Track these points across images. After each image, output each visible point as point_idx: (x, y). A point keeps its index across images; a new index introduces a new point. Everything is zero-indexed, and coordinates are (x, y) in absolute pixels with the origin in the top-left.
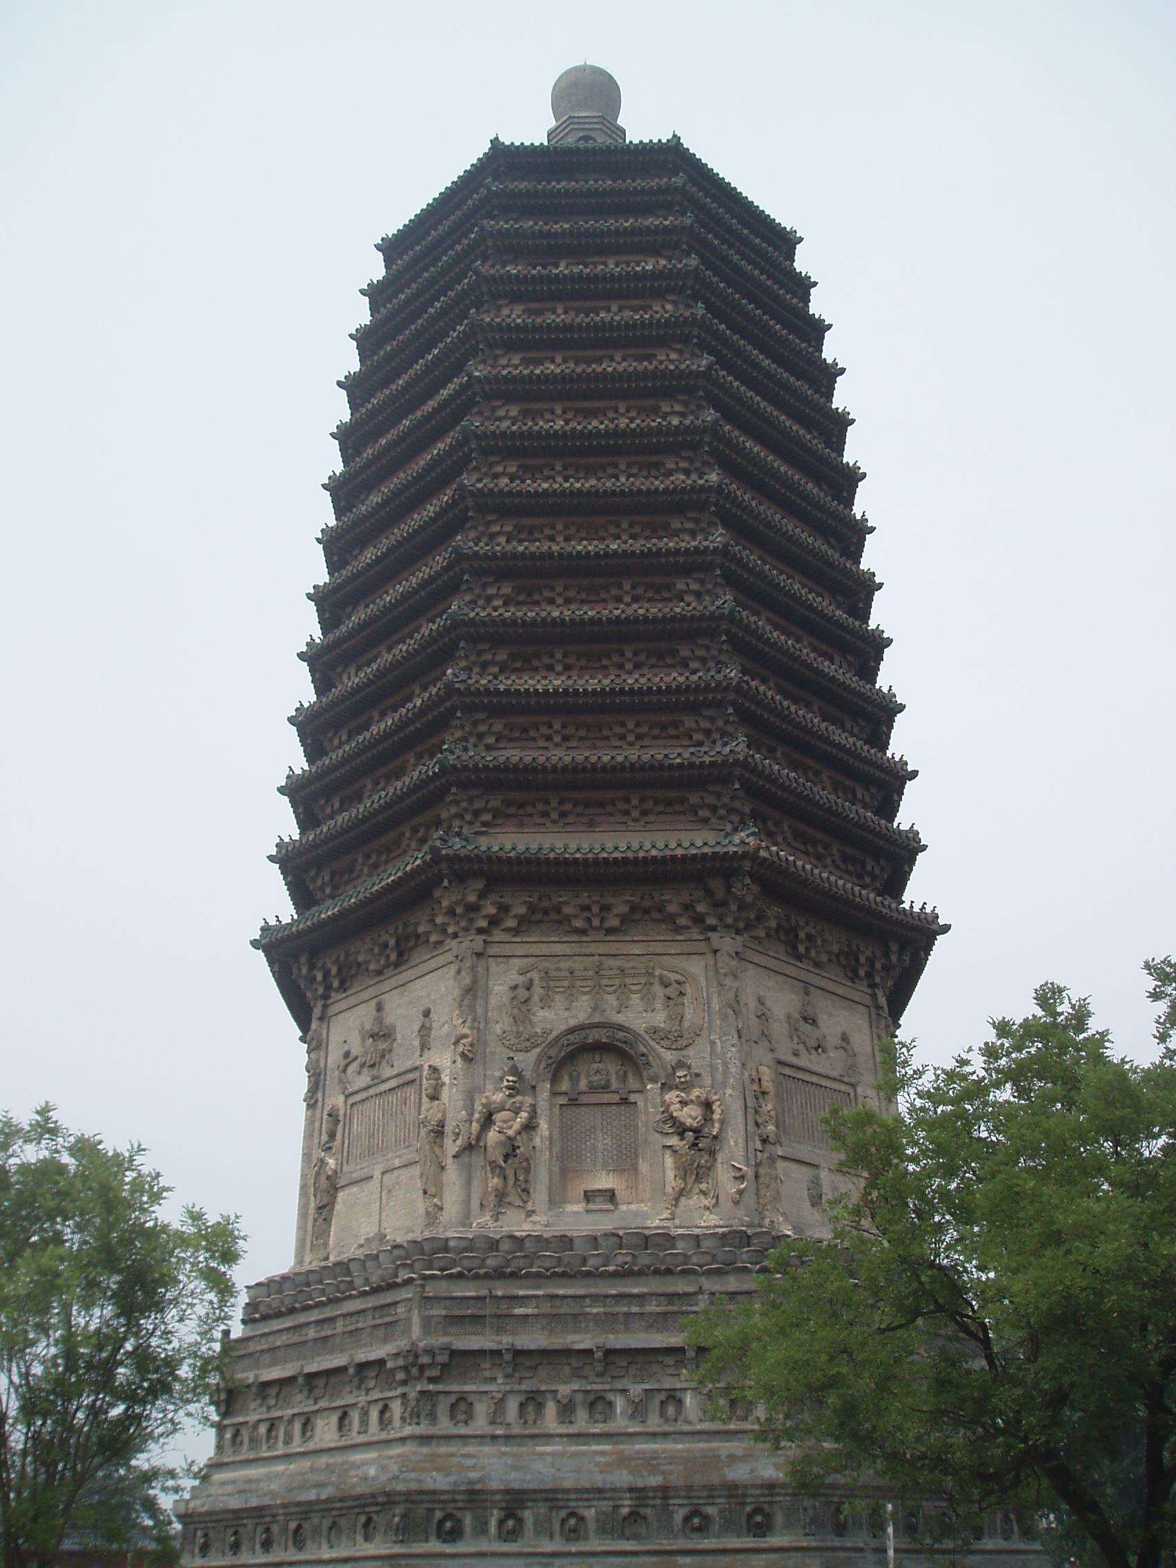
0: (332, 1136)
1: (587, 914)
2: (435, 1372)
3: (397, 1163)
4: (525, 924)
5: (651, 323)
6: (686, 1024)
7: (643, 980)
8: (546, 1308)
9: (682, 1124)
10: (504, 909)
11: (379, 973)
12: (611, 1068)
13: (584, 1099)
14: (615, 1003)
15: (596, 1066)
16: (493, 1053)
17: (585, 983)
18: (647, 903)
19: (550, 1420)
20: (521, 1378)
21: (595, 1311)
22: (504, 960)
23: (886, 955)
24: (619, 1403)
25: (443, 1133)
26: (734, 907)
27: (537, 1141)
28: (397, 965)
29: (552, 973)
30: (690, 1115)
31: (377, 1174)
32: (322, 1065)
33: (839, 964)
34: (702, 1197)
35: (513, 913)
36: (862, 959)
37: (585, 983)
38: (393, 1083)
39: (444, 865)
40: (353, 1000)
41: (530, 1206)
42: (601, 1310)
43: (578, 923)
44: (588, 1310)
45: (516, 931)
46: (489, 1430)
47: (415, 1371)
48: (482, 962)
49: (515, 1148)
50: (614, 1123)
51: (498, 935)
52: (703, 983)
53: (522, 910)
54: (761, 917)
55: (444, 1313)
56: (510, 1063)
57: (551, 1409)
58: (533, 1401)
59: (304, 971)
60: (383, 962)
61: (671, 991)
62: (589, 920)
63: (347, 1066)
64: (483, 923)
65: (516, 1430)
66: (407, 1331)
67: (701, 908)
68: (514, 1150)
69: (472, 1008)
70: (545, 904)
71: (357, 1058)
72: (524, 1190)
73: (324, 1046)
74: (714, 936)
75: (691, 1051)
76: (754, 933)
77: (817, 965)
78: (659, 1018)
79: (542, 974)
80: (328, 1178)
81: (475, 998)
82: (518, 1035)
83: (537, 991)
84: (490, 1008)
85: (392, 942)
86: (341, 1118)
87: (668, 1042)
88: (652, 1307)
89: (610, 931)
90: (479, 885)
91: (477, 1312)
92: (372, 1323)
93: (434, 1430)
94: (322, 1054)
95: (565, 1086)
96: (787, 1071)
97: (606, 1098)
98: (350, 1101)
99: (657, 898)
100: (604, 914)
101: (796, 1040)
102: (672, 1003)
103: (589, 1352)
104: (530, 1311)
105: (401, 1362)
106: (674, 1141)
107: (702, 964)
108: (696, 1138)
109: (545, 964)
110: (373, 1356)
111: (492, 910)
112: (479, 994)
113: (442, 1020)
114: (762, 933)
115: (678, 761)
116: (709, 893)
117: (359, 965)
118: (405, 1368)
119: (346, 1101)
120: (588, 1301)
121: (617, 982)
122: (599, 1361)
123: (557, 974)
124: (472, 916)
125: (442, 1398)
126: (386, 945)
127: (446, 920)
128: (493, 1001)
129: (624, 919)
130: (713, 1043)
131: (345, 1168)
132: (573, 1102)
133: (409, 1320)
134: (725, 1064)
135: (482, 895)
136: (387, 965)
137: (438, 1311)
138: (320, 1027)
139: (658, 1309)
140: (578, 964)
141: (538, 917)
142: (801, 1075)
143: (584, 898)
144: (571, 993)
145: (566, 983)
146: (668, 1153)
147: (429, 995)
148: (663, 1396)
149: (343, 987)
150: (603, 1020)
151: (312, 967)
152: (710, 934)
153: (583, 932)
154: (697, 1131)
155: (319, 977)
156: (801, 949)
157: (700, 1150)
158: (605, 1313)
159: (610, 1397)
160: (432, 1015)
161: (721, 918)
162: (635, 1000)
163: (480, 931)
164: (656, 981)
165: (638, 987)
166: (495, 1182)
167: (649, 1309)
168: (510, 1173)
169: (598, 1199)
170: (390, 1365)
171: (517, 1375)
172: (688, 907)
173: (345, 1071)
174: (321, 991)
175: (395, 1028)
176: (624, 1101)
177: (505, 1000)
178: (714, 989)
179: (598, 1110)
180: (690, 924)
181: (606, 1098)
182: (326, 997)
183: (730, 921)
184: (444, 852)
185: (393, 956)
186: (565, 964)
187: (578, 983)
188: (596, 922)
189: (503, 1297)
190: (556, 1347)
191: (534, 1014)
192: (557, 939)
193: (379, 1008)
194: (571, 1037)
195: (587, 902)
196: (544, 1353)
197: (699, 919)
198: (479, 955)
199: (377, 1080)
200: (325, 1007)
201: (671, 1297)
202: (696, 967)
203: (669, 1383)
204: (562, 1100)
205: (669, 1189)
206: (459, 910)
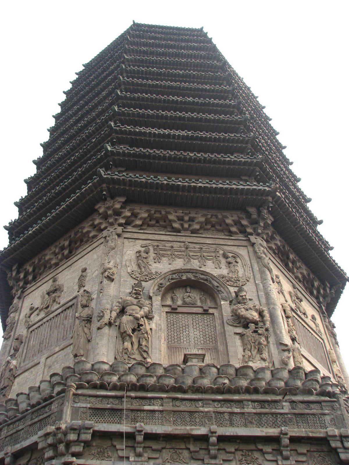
0: (16, 350)
3: (57, 349)
4: (146, 224)
5: (198, 55)
7: (213, 254)
8: (169, 406)
9: (246, 318)
10: (135, 215)
11: (57, 264)
12: (195, 296)
13: (180, 310)
14: (198, 264)
15: (188, 294)
17: (180, 253)
18: (214, 220)
20: (149, 458)
21: (206, 410)
22: (134, 240)
23: (324, 289)
25: (91, 322)
26: (262, 224)
28: (67, 257)
31: (43, 360)
32: (16, 319)
34: (262, 362)
35: (139, 217)
37: (180, 253)
38: (60, 311)
39: (104, 185)
42: (211, 409)
43: (176, 225)
44: (201, 409)
45: (140, 227)
47: (62, 447)
48: (119, 241)
49: (140, 325)
50: (200, 324)
51: (130, 228)
52: (247, 258)
55: (89, 406)
59: (14, 274)
60: (60, 257)
62: (182, 225)
63: (31, 314)
64: (123, 221)
67: (245, 222)
68: (139, 327)
70: (158, 215)
71: (37, 308)
72: (145, 351)
73: (19, 311)
74: (253, 239)
77: (297, 277)
78: (224, 271)
79: (155, 247)
80: (11, 370)
83: (152, 254)
84: (124, 260)
86: (24, 341)
88: (249, 409)
89: (194, 232)
90: (123, 199)
91: (115, 407)
92: (30, 423)
94: (17, 314)
97: (194, 310)
98: (31, 329)
99: (220, 217)
100: (191, 223)
102: (231, 265)
103: (204, 438)
104: (156, 408)
105: (50, 440)
106: (239, 330)
107: (246, 251)
108: (256, 328)
109: (156, 243)
111: (128, 214)
113: (93, 271)
115: (228, 159)
116: (249, 216)
118: (54, 446)
119: (28, 331)
122: (214, 445)
124: (116, 217)
127: (101, 221)
128: (126, 258)
131: (22, 364)
132: (173, 311)
135: (122, 208)
136: (61, 260)
138: (18, 302)
139: (254, 411)
140: (176, 245)
141: (153, 222)
143: (180, 213)
144: (173, 257)
146: (238, 337)
147: (86, 263)
149: (34, 279)
150: (192, 268)
151: (18, 273)
153: (179, 231)
155: (22, 275)
157: (259, 334)
158: (214, 412)
160: (87, 271)
161: (254, 229)
163: (120, 225)
164: (221, 256)
165: (211, 258)
167: (246, 410)
169: (194, 360)
170: (40, 446)
171: (146, 455)
172: (237, 223)
173: (29, 317)
174: (21, 284)
175: (63, 285)
176: (206, 312)
177: (134, 257)
178: (254, 261)
179: (190, 317)
181: (194, 310)
182: (24, 288)
183: (260, 231)
185: (66, 252)
186: (169, 245)
187: (176, 253)
188: (186, 226)
189: (136, 398)
190: (177, 432)
191: (150, 265)
192: (164, 233)
193: (54, 281)
194: (174, 276)
195: (182, 215)
196: (169, 438)
197: (243, 231)
199: (47, 315)
201: (262, 403)
202: (243, 252)
204: (167, 309)
206: (110, 212)
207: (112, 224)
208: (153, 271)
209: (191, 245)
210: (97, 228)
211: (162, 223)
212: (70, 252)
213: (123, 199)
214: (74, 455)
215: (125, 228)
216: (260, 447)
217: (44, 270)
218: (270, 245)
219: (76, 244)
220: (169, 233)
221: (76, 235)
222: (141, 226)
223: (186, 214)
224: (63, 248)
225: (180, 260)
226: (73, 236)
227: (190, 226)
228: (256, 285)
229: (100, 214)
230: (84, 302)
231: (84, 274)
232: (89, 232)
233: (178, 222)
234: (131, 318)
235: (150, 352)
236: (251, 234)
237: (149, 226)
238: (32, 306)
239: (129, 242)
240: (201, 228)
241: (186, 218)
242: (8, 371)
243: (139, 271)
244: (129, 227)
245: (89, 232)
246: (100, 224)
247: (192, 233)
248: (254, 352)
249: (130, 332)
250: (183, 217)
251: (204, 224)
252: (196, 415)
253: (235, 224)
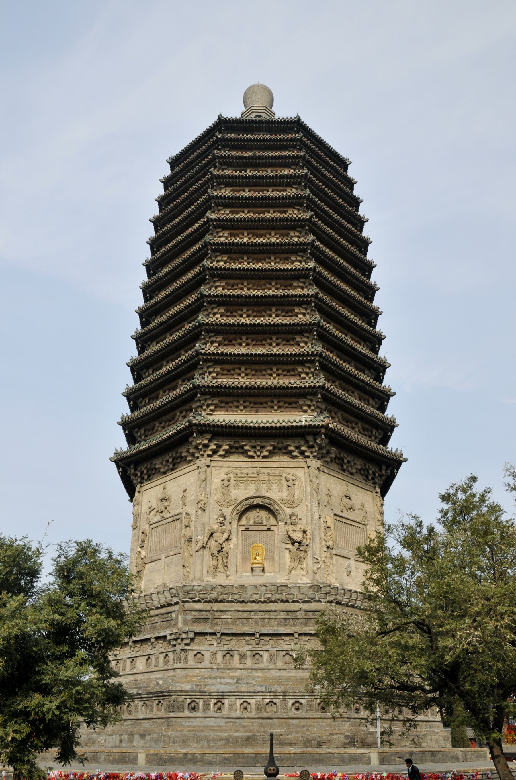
2: (188, 641)
3: (172, 553)
4: (228, 453)
6: (296, 497)
7: (278, 478)
9: (293, 540)
10: (219, 446)
11: (165, 473)
12: (263, 514)
16: (213, 508)
17: (253, 479)
18: (280, 446)
19: (236, 661)
23: (381, 470)
24: (265, 655)
26: (317, 449)
27: (232, 546)
28: (172, 470)
29: (239, 475)
30: (297, 536)
31: (163, 557)
33: (361, 474)
36: (370, 472)
38: (170, 519)
40: (153, 484)
41: (228, 573)
43: (250, 453)
46: (209, 666)
48: (209, 469)
49: (222, 548)
51: (216, 458)
52: (303, 479)
54: (328, 453)
56: (221, 512)
57: (236, 657)
58: (229, 653)
59: (132, 471)
61: (289, 483)
62: (255, 452)
65: (222, 666)
66: (176, 624)
67: (303, 448)
69: (205, 488)
70: (237, 445)
75: (297, 509)
76: (326, 459)
77: (352, 474)
78: (284, 495)
80: (142, 559)
81: (206, 483)
82: (224, 500)
83: (232, 481)
84: (212, 488)
85: (171, 460)
87: (288, 505)
89: (264, 457)
90: (209, 436)
93: (186, 666)
95: (243, 522)
96: (338, 518)
97: (261, 528)
98: (152, 526)
101: (342, 505)
105: (173, 637)
106: (290, 546)
107: (303, 472)
109: (236, 471)
110: (162, 634)
111: (214, 447)
112: (208, 483)
114: (329, 460)
116: (307, 442)
117: (156, 469)
118: (175, 640)
120: (253, 613)
121: (267, 479)
123: (241, 475)
125: (190, 652)
126: (168, 461)
127: (194, 451)
128: (213, 486)
129: (270, 452)
130: (307, 506)
133: (177, 619)
134: (312, 515)
135: (210, 441)
136: (168, 470)
137: (190, 616)
140: (250, 471)
142: (344, 520)
145: (245, 479)
146: (287, 551)
147: (186, 483)
148: (284, 653)
149: (149, 478)
151: (136, 470)
152: (307, 459)
154: (300, 543)
155: (139, 474)
156: (345, 467)
159: (261, 653)
161: (312, 452)
162: (274, 487)
163: (209, 456)
164: (284, 479)
166: (215, 562)
168: (220, 558)
176: (269, 529)
177: (219, 485)
178: (308, 483)
180: (298, 455)
181: (261, 528)
183: (315, 454)
184: (194, 422)
185: (171, 466)
186: (245, 471)
187: (250, 479)
194: (247, 502)
195: (255, 444)
197: (302, 453)
198: (208, 466)
200: (141, 487)
202: (301, 474)
203: (286, 648)
205: (287, 567)
206: (200, 447)
208: (233, 498)
213: (209, 436)
214: (186, 645)
216: (283, 638)
218: (326, 459)
221: (177, 453)
225: (253, 485)
228: (307, 506)
230: (187, 524)
231: (185, 494)
234: (217, 544)
235: (229, 566)
236: (308, 457)
238: (150, 504)
239: (216, 470)
242: (140, 559)
243: (223, 498)
248: (296, 563)
249: (216, 554)
252: (250, 620)
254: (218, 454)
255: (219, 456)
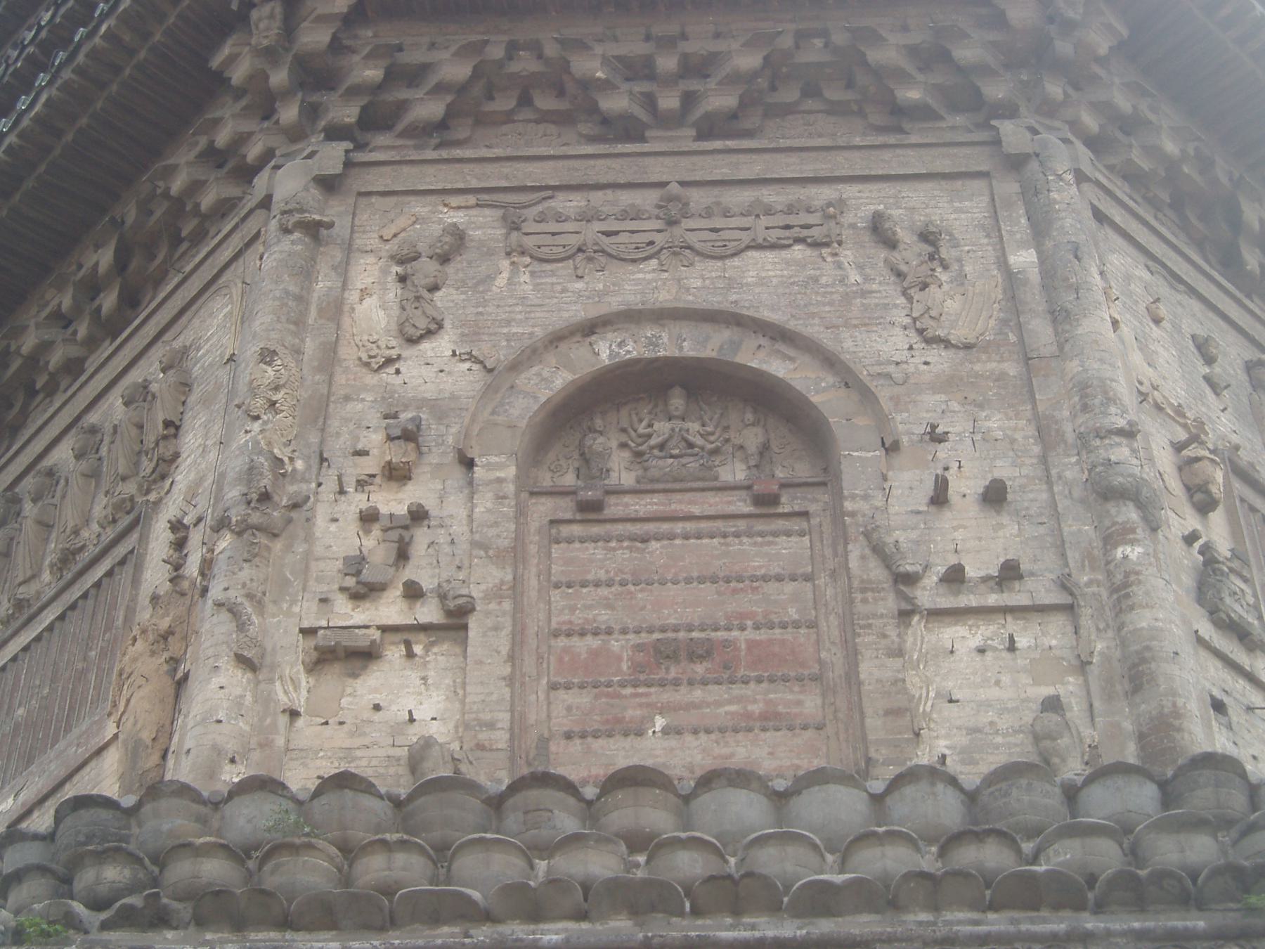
1: (641, 87)
11: (74, 368)
43: (615, 103)
51: (383, 145)
53: (458, 71)
60: (82, 330)
74: (1012, 133)
100: (694, 85)
127: (245, 126)
136: (92, 343)
163: (334, 133)
185: (109, 301)
206: (279, 78)
207: (296, 134)
209: (698, 198)
210: (230, 165)
211: (545, 102)
212: (131, 301)
215: (360, 147)
217: (25, 406)
219: (152, 257)
220: (589, 149)
222: (442, 126)
223: (668, 43)
224: (93, 287)
226: (131, 214)
227: (689, 99)
229: (239, 93)
232: (196, 187)
233: (625, 86)
236: (1009, 111)
237: (482, 120)
240: (745, 103)
241: (667, 63)
244: (381, 139)
245: (196, 187)
246: (241, 140)
247: (700, 137)
250: (648, 61)
251: (763, 83)
253: (925, 68)
254: (400, 127)
255: (404, 134)
